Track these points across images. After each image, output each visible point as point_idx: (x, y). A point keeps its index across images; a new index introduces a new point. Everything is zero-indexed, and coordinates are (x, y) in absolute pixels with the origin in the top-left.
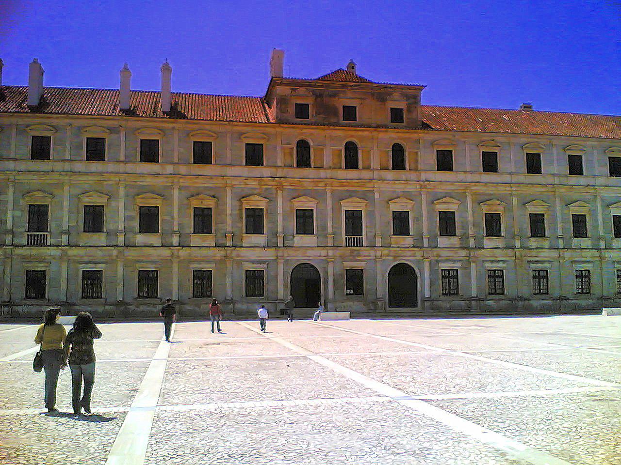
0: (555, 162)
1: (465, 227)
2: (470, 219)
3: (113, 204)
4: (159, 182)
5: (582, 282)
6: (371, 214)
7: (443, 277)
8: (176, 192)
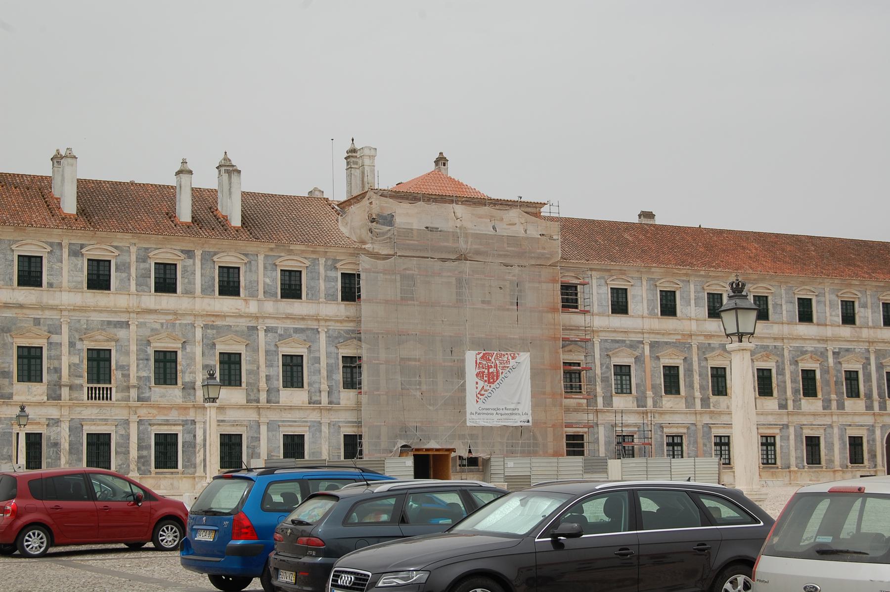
0: (693, 302)
3: (188, 350)
4: (244, 323)
5: (721, 450)
8: (262, 334)
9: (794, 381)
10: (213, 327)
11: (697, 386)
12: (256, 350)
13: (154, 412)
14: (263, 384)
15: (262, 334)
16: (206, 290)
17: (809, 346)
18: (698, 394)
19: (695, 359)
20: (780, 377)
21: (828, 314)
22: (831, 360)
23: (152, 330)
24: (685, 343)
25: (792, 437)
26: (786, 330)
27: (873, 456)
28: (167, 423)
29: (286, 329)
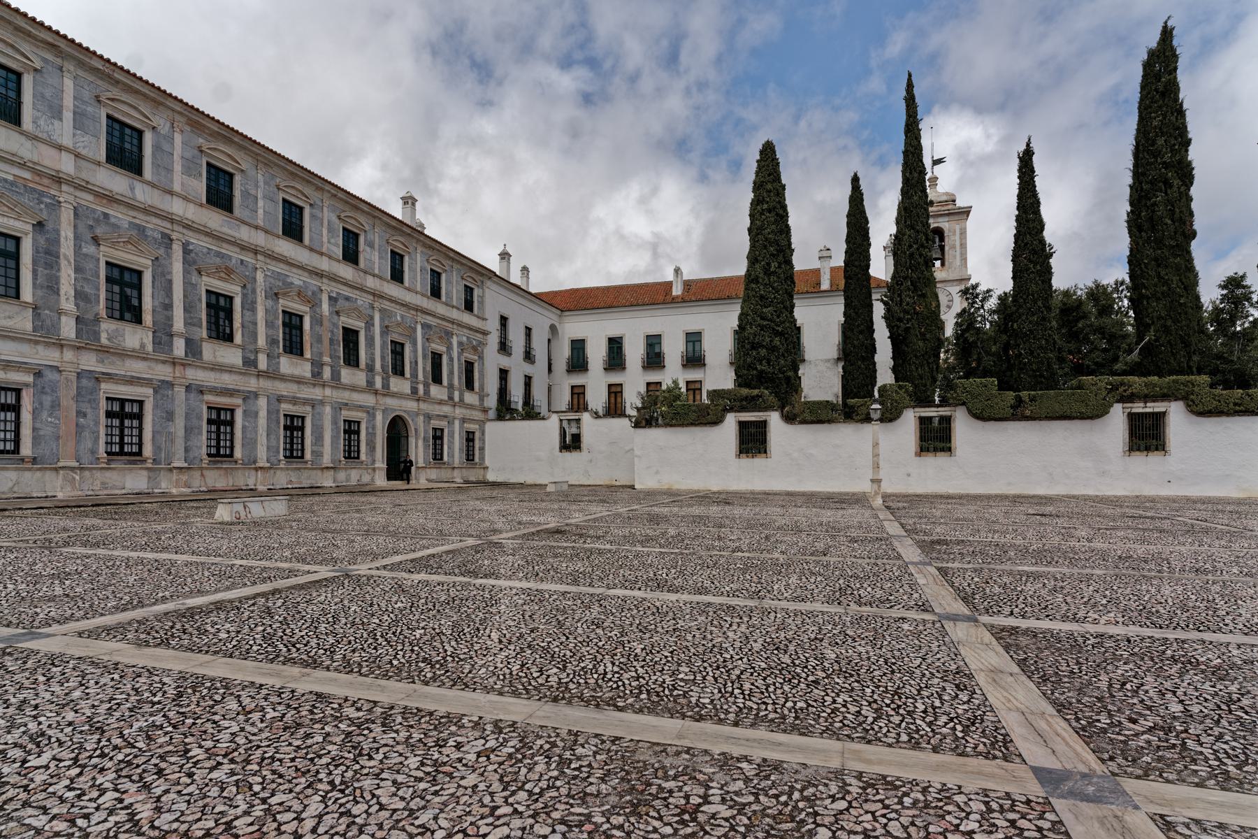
0: (68, 115)
9: (270, 325)
24: (42, 194)
25: (263, 414)
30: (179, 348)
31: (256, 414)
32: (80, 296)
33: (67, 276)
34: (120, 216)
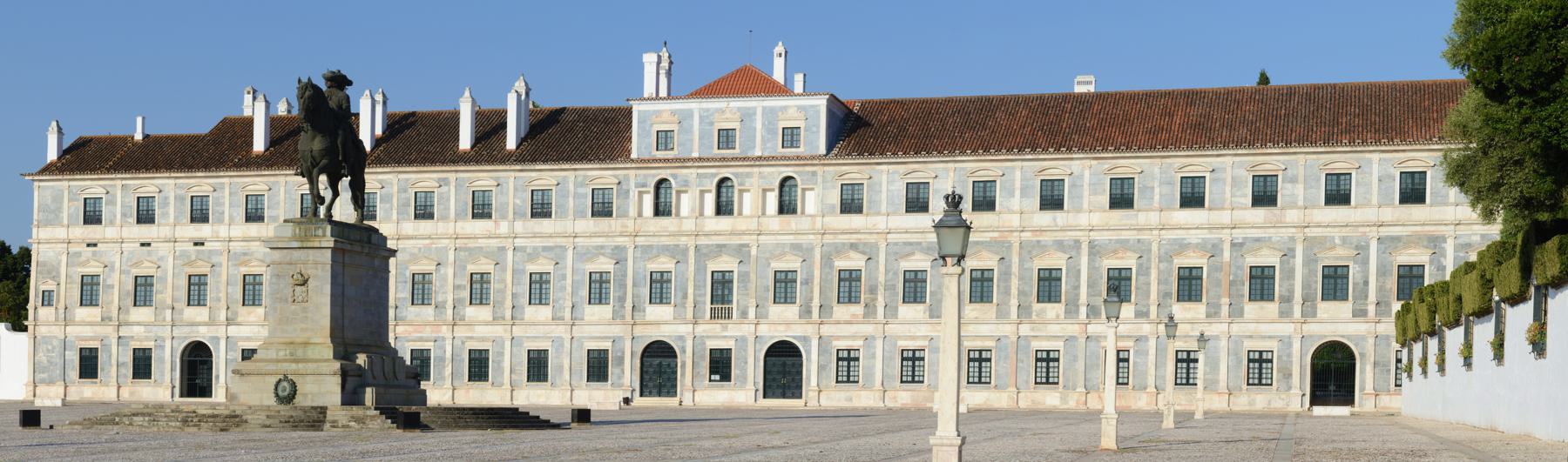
1: (873, 290)
2: (882, 279)
4: (494, 243)
6: (744, 277)
7: (839, 359)
10: (466, 249)
11: (1014, 292)
12: (504, 270)
13: (410, 329)
14: (509, 304)
15: (510, 253)
16: (459, 216)
17: (1194, 237)
18: (1014, 302)
19: (1015, 260)
20: (1141, 278)
21: (1228, 194)
22: (1227, 254)
23: (412, 254)
26: (1153, 218)
27: (1288, 376)
28: (421, 339)
29: (535, 248)
30: (1083, 310)
31: (1147, 354)
32: (1021, 293)
33: (1015, 283)
34: (1047, 238)
